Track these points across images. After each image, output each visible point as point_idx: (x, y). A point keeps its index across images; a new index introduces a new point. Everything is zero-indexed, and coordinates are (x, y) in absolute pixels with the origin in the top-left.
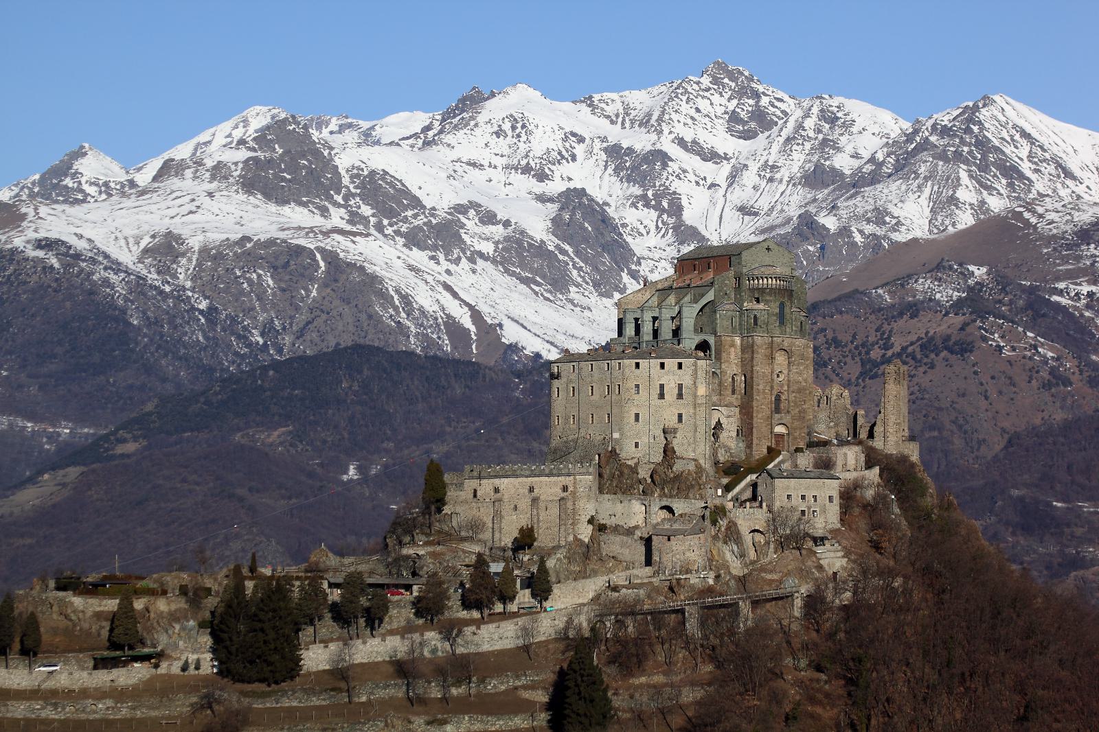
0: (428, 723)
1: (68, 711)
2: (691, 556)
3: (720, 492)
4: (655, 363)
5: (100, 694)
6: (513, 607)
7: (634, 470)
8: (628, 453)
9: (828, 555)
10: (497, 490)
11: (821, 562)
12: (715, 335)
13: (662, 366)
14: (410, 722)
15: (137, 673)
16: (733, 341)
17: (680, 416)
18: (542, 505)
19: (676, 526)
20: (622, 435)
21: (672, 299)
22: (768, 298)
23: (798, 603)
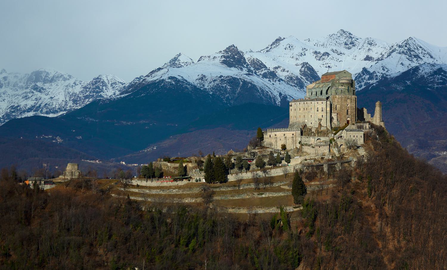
3: (333, 135)
4: (316, 102)
6: (280, 165)
7: (311, 130)
8: (309, 125)
10: (276, 135)
11: (359, 153)
13: (318, 103)
15: (185, 182)
17: (322, 116)
18: (287, 139)
22: (345, 85)
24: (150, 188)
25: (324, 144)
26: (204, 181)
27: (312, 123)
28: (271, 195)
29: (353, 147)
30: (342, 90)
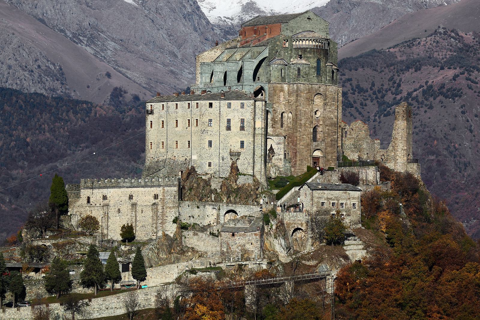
2: (248, 247)
4: (224, 103)
6: (117, 286)
7: (207, 183)
10: (105, 198)
11: (347, 253)
17: (242, 143)
18: (139, 209)
19: (239, 225)
25: (248, 226)
27: (211, 162)
29: (332, 234)
30: (299, 69)
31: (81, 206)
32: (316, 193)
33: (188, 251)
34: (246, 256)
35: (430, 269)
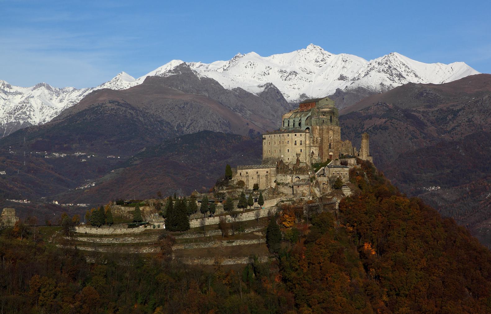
0: (228, 243)
1: (120, 241)
2: (304, 191)
5: (130, 235)
6: (252, 208)
7: (288, 166)
8: (286, 161)
9: (345, 191)
10: (247, 173)
11: (344, 193)
12: (311, 126)
14: (222, 242)
15: (141, 228)
16: (317, 127)
17: (301, 150)
18: (260, 177)
19: (301, 183)
20: (284, 156)
21: (298, 115)
23: (337, 205)
24: (101, 236)
25: (304, 183)
26: (164, 227)
27: (289, 158)
28: (242, 243)
29: (337, 185)
30: (323, 120)
31: (238, 176)
32: (331, 169)
33: (280, 194)
34: (304, 195)
35: (377, 199)
